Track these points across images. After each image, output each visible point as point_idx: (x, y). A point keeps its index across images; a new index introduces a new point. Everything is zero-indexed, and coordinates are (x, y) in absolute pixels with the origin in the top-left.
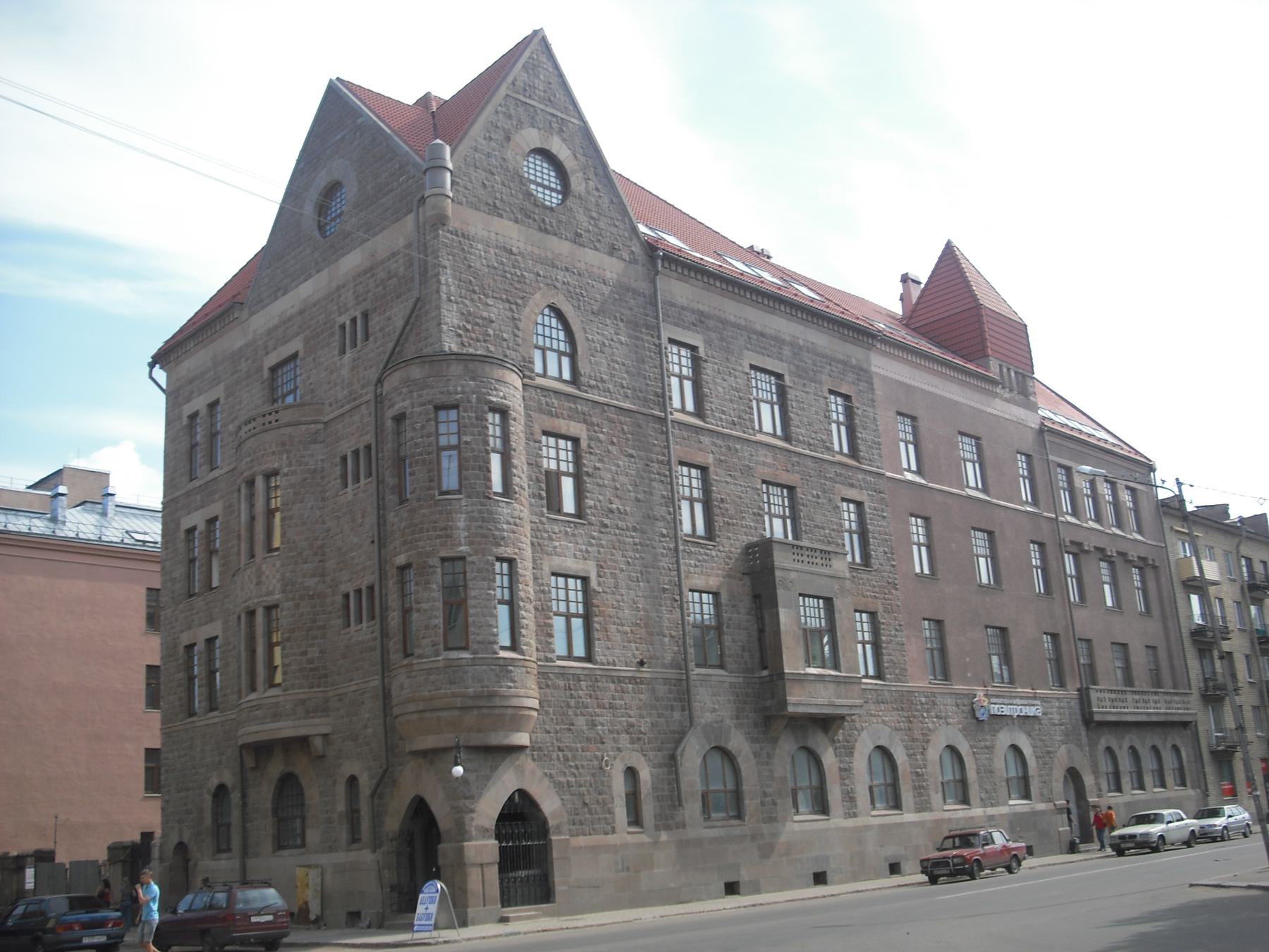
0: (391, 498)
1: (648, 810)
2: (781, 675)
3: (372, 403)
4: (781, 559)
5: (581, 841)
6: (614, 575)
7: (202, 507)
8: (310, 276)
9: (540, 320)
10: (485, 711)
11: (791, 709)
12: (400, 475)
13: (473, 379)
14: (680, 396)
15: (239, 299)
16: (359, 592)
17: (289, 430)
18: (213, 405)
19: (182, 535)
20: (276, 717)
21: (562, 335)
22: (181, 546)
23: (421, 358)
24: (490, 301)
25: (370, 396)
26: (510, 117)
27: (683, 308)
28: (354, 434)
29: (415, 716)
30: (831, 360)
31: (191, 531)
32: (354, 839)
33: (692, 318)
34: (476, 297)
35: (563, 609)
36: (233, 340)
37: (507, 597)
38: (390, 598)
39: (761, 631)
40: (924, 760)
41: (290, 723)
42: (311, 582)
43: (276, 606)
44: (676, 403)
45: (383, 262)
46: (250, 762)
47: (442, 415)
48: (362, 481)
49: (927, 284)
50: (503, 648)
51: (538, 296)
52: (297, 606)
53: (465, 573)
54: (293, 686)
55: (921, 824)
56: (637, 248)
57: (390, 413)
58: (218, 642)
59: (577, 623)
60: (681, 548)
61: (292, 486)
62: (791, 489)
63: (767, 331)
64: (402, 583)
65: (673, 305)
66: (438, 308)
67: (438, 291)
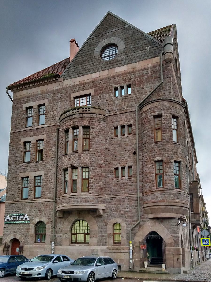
8: (98, 71)
45: (139, 71)
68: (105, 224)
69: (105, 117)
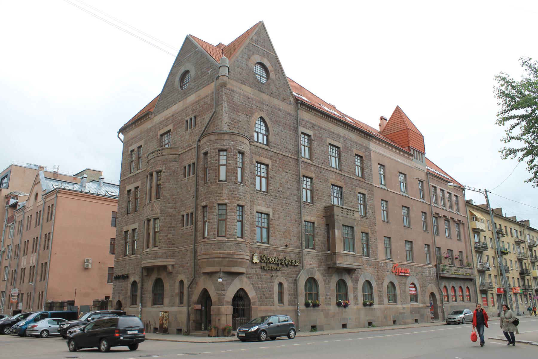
0: (201, 182)
1: (286, 298)
2: (335, 253)
3: (196, 149)
4: (337, 211)
5: (263, 308)
6: (278, 214)
7: (134, 182)
8: (176, 103)
9: (257, 122)
10: (231, 259)
11: (338, 265)
12: (205, 174)
13: (233, 141)
14: (305, 152)
15: (150, 111)
16: (188, 215)
17: (166, 156)
18: (140, 147)
19: (126, 192)
20: (156, 258)
21: (264, 128)
22: (126, 196)
23: (214, 133)
24: (240, 114)
25: (196, 146)
26: (250, 50)
27: (307, 122)
28: (189, 159)
29: (206, 260)
30: (357, 144)
31: (129, 191)
32: (181, 303)
33: (310, 125)
34: (235, 112)
35: (260, 225)
36: (147, 125)
37: (240, 219)
38: (199, 217)
39: (328, 237)
40: (382, 286)
41: (160, 260)
42: (171, 210)
43: (158, 218)
44: (303, 155)
45: (203, 99)
46: (145, 274)
47: (221, 153)
48: (191, 176)
49: (389, 120)
50: (238, 237)
51: (257, 114)
52: (165, 219)
53: (226, 210)
54: (162, 247)
55: (380, 309)
56: (292, 100)
57: (203, 151)
58: (136, 231)
59: (265, 231)
60: (302, 206)
61: (166, 176)
62: (341, 188)
63: (335, 132)
64: (204, 212)
65: (303, 120)
66: (221, 115)
67: (222, 110)
68: (173, 282)
69: (177, 156)
